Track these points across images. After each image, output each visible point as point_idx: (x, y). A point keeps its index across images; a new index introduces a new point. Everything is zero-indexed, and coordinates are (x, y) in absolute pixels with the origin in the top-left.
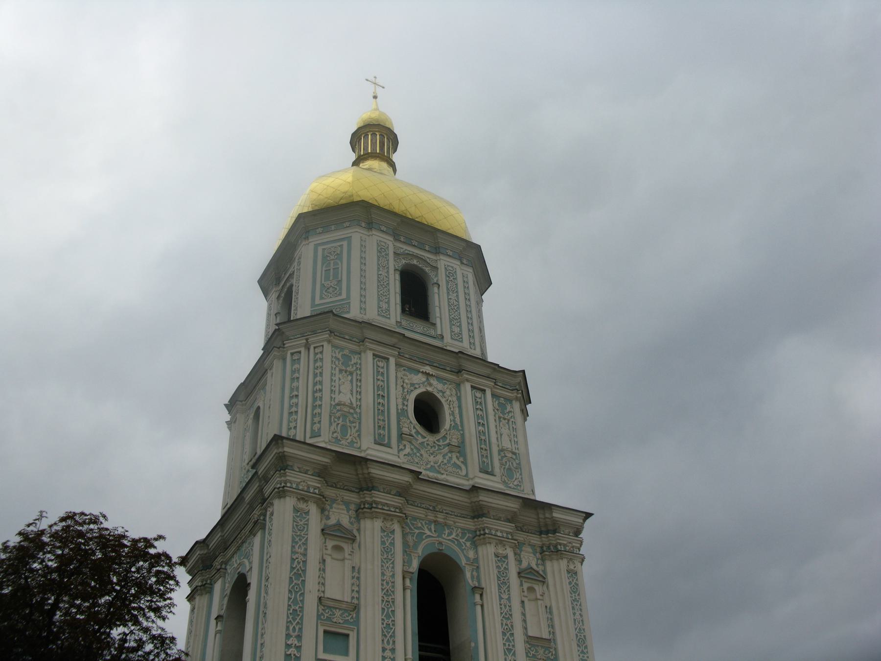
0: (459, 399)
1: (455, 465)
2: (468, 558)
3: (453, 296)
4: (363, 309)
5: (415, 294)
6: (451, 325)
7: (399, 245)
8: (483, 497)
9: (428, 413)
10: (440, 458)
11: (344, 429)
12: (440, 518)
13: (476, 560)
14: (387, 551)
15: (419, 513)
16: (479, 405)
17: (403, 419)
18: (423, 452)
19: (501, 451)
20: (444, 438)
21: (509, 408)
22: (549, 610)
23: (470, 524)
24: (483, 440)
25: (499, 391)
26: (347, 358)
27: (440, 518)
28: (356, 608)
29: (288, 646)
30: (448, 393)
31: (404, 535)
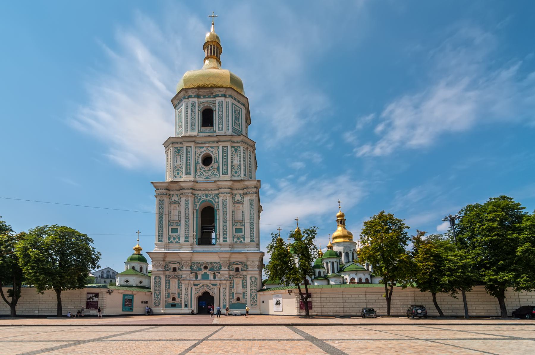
0: (219, 152)
1: (216, 175)
2: (215, 202)
3: (220, 113)
4: (186, 131)
5: (207, 117)
6: (219, 125)
7: (200, 100)
8: (219, 183)
9: (207, 160)
10: (210, 173)
11: (178, 174)
12: (207, 192)
13: (218, 202)
14: (187, 204)
15: (199, 192)
16: (225, 152)
17: (197, 165)
18: (204, 173)
19: (232, 167)
20: (212, 167)
21: (238, 149)
22: (243, 212)
23: (217, 192)
24: (225, 164)
25: (234, 145)
26: (179, 150)
27: (207, 192)
28: (180, 221)
29: (159, 234)
30: (214, 151)
31: (194, 200)
